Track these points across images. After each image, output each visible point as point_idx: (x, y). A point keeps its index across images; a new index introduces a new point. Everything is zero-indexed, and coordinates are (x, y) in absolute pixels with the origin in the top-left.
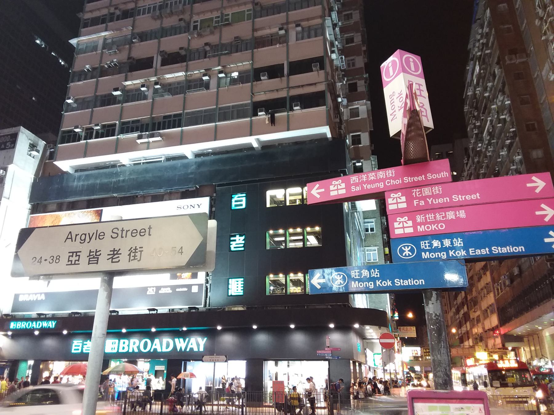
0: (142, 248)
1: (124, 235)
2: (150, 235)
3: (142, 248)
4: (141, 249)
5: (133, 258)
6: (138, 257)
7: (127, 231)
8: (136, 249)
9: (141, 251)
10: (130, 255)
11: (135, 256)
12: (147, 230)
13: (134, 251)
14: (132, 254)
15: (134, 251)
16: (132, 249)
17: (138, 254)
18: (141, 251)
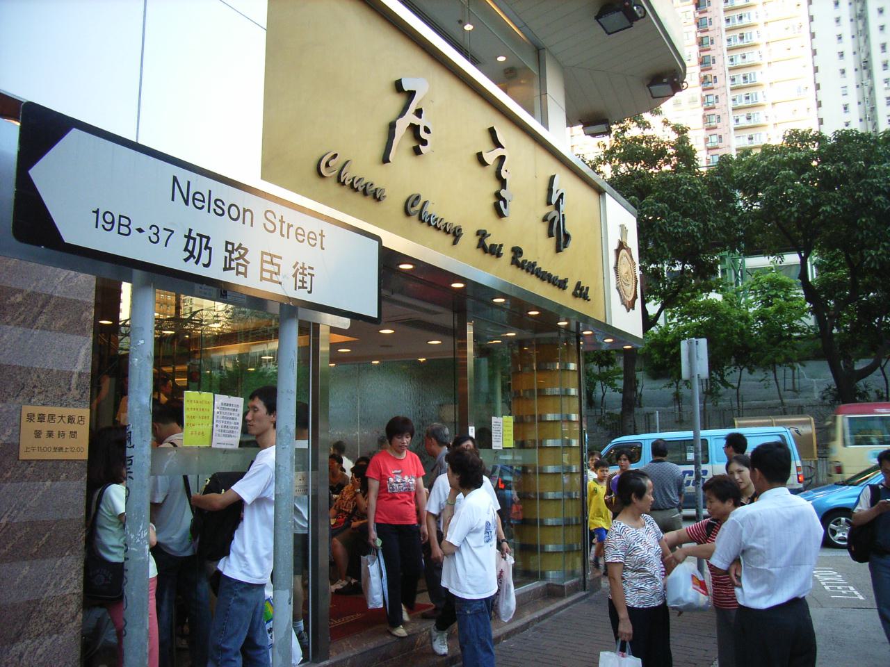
0: (312, 269)
1: (285, 232)
2: (323, 249)
3: (312, 269)
5: (300, 284)
6: (308, 285)
7: (290, 226)
8: (303, 268)
9: (312, 275)
10: (295, 276)
11: (303, 281)
12: (319, 238)
13: (301, 271)
14: (299, 277)
15: (301, 271)
16: (298, 267)
17: (307, 279)
18: (312, 275)
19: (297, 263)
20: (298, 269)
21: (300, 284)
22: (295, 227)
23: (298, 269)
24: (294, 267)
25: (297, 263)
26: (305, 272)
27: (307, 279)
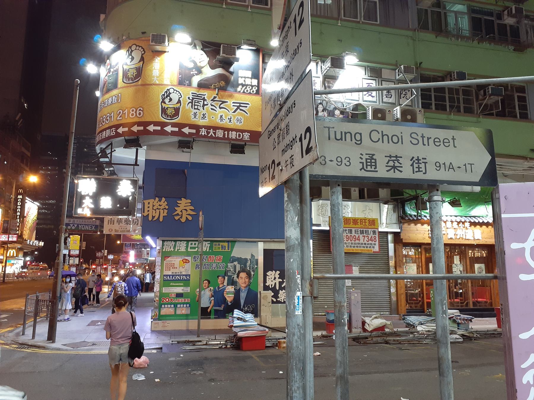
0: (425, 159)
3: (425, 159)
4: (425, 161)
8: (418, 159)
9: (425, 163)
14: (416, 165)
16: (414, 159)
17: (422, 166)
18: (425, 163)
19: (413, 158)
20: (414, 161)
21: (417, 170)
22: (433, 139)
23: (414, 161)
24: (411, 160)
25: (413, 158)
26: (420, 162)
27: (422, 166)
